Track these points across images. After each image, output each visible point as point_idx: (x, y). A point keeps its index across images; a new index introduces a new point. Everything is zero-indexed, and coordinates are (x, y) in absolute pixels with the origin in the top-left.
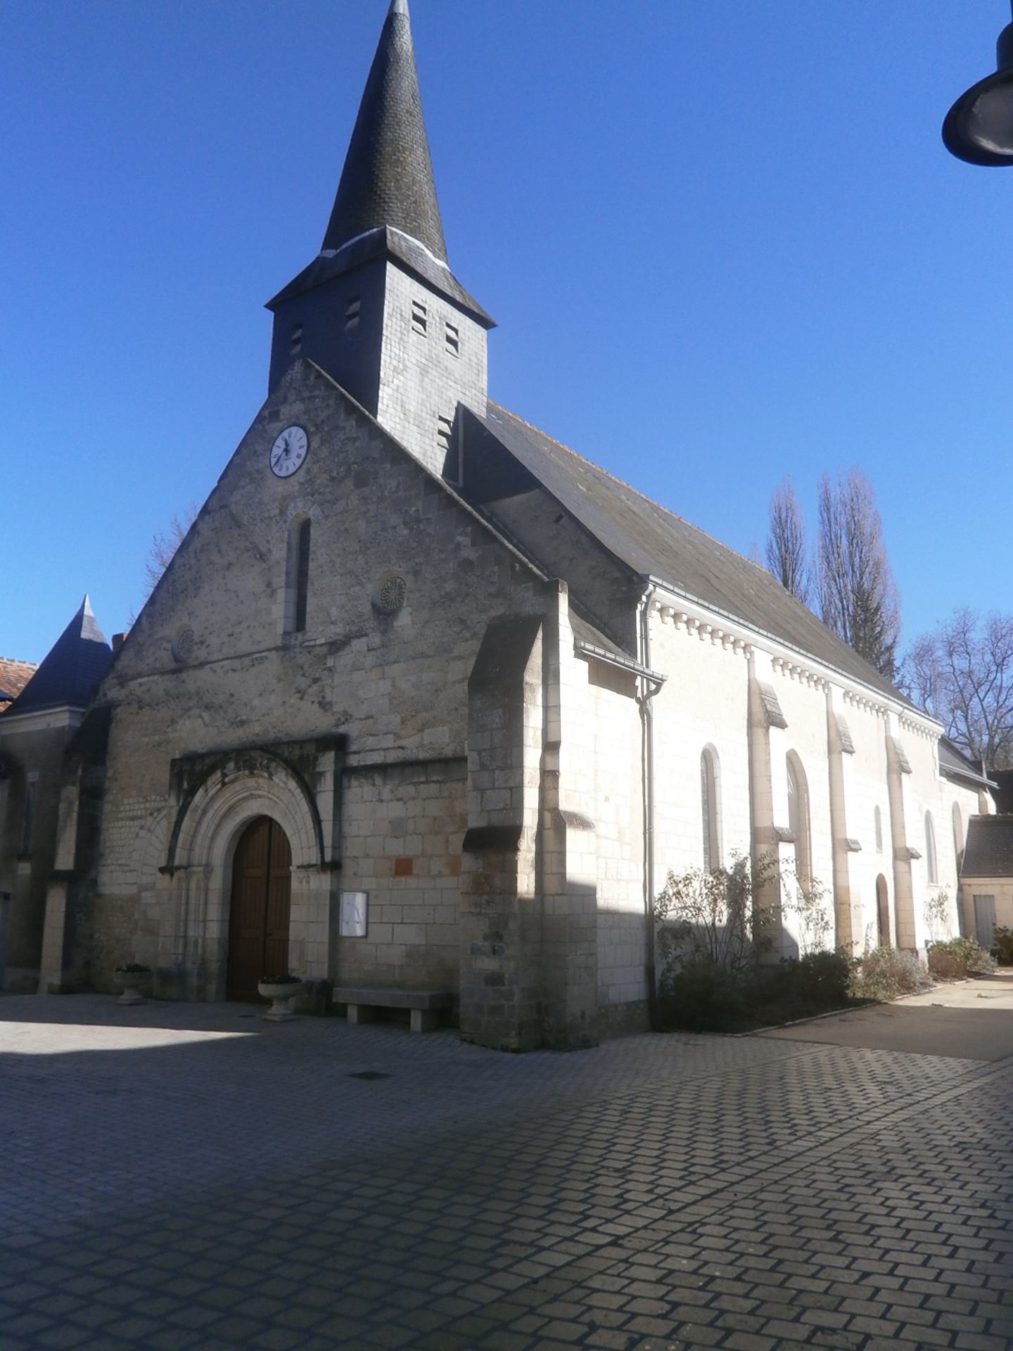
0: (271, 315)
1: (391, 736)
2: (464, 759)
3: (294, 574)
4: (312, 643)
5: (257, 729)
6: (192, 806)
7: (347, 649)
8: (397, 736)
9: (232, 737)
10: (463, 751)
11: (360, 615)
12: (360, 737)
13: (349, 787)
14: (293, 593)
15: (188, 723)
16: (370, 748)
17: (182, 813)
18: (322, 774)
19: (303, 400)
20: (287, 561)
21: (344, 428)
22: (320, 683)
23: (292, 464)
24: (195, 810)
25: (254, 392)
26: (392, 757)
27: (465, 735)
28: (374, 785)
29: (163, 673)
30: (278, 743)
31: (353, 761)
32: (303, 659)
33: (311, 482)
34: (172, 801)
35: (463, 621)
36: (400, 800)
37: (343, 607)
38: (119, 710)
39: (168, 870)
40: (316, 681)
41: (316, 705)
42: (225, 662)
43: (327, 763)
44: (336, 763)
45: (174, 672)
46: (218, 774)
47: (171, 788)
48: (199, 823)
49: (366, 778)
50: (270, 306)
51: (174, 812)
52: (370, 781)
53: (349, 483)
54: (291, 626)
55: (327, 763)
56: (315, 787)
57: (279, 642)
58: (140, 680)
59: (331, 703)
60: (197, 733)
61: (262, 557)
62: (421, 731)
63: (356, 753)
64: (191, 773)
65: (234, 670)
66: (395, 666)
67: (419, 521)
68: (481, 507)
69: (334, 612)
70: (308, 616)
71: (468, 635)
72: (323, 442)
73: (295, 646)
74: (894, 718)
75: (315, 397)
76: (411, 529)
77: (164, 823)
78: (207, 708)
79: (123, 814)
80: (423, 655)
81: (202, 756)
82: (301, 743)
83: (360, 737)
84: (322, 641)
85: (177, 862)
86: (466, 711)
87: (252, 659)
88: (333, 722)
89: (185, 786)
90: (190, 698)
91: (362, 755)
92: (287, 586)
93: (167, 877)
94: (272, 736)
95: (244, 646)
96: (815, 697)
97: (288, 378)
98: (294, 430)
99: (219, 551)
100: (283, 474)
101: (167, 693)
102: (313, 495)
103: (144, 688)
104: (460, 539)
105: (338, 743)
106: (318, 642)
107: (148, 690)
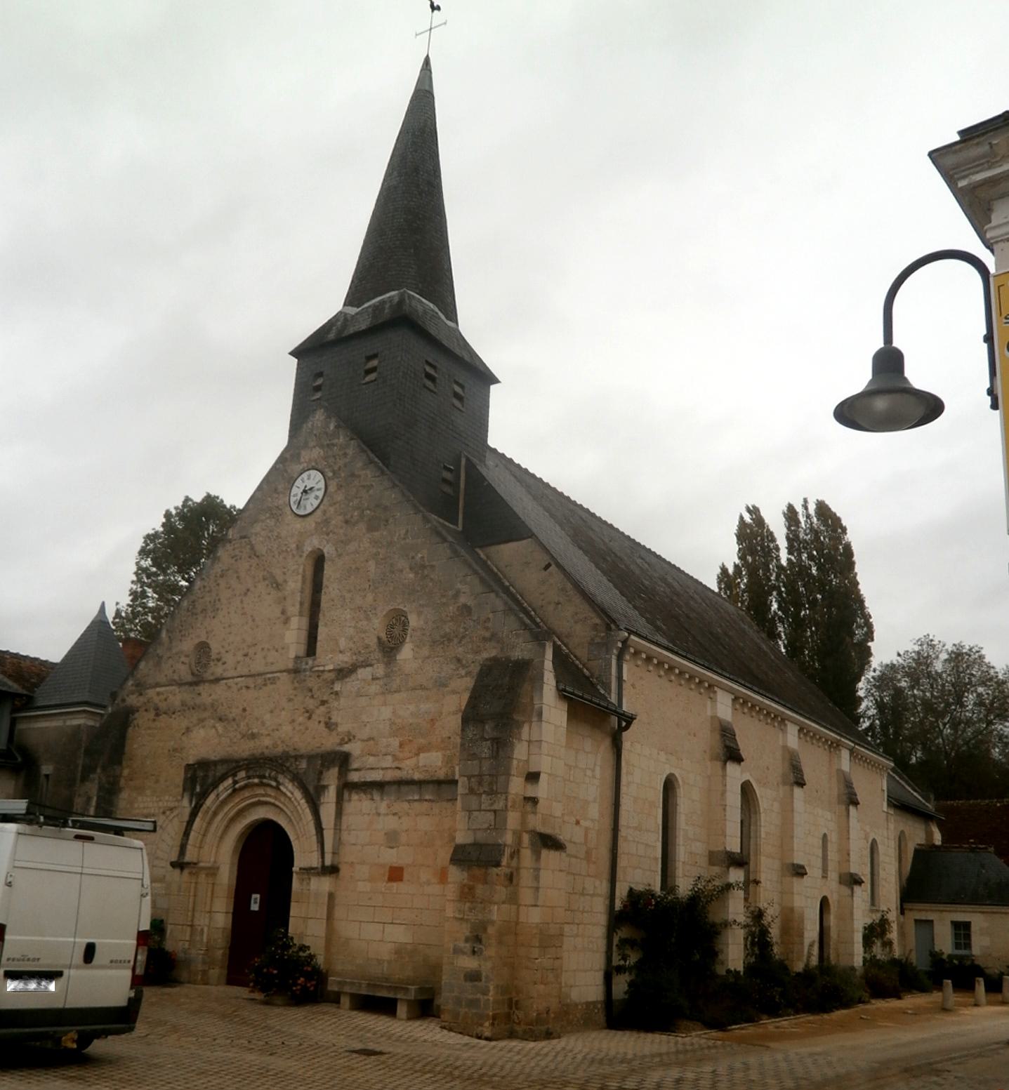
0: (294, 361)
1: (389, 758)
2: (455, 782)
3: (307, 605)
4: (321, 668)
5: (267, 742)
6: (205, 807)
7: (353, 677)
8: (395, 758)
9: (245, 749)
10: (453, 774)
11: (367, 647)
12: (362, 756)
13: (350, 800)
14: (305, 622)
15: (202, 732)
16: (368, 767)
17: (194, 814)
18: (325, 787)
19: (322, 446)
20: (302, 592)
21: (359, 476)
22: (326, 705)
23: (311, 503)
24: (207, 812)
25: (276, 438)
26: (390, 776)
27: (456, 761)
28: (372, 799)
29: (180, 684)
30: (286, 756)
31: (354, 777)
32: (312, 682)
33: (326, 522)
34: (186, 802)
35: (459, 660)
36: (395, 814)
37: (351, 638)
38: (137, 715)
39: (179, 865)
40: (323, 703)
41: (322, 724)
42: (239, 679)
43: (331, 779)
44: (339, 779)
45: (191, 684)
46: (230, 781)
47: (184, 790)
48: (210, 823)
49: (365, 793)
50: (296, 353)
51: (187, 811)
52: (369, 796)
53: (362, 526)
54: (302, 650)
55: (331, 779)
56: (319, 798)
57: (291, 665)
58: (158, 689)
59: (336, 724)
60: (205, 742)
61: (278, 586)
62: (417, 755)
63: (356, 770)
64: (201, 779)
65: (248, 688)
66: (396, 696)
67: (423, 567)
68: (478, 550)
69: (343, 643)
70: (318, 644)
71: (463, 672)
72: (340, 487)
73: (305, 670)
74: (845, 754)
75: (333, 445)
76: (416, 573)
77: (176, 821)
78: (220, 719)
79: (137, 811)
80: (422, 688)
81: (215, 763)
82: (311, 758)
83: (362, 756)
84: (331, 667)
85: (187, 858)
86: (459, 741)
87: (263, 679)
88: (338, 741)
89: (198, 789)
90: (205, 709)
91: (362, 772)
92: (301, 614)
93: (177, 871)
94: (280, 749)
95: (258, 666)
96: (773, 740)
97: (310, 424)
98: (313, 472)
99: (238, 577)
100: (302, 512)
101: (183, 704)
102: (328, 534)
103: (162, 697)
104: (459, 586)
105: (343, 760)
106: (327, 668)
107: (166, 700)
